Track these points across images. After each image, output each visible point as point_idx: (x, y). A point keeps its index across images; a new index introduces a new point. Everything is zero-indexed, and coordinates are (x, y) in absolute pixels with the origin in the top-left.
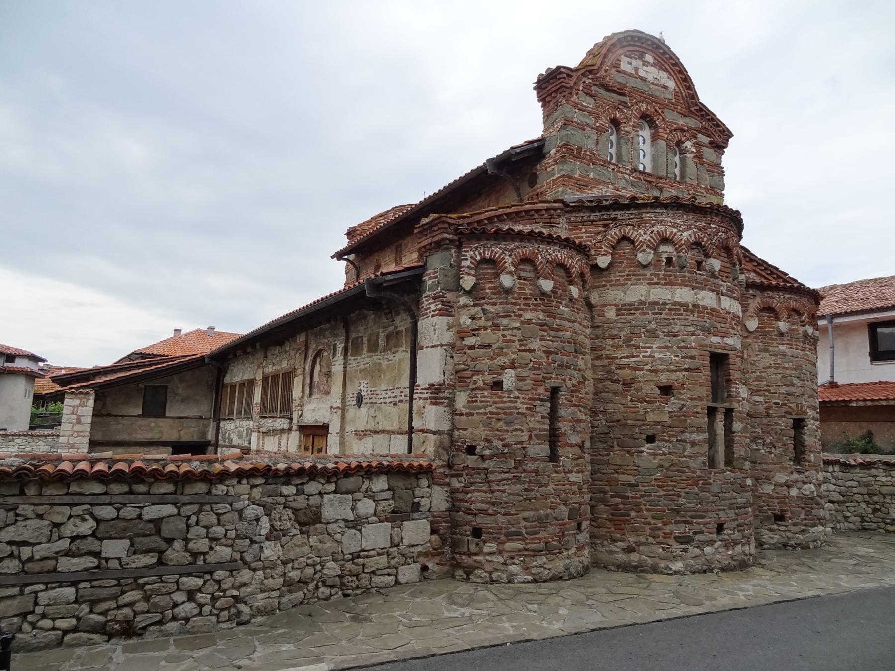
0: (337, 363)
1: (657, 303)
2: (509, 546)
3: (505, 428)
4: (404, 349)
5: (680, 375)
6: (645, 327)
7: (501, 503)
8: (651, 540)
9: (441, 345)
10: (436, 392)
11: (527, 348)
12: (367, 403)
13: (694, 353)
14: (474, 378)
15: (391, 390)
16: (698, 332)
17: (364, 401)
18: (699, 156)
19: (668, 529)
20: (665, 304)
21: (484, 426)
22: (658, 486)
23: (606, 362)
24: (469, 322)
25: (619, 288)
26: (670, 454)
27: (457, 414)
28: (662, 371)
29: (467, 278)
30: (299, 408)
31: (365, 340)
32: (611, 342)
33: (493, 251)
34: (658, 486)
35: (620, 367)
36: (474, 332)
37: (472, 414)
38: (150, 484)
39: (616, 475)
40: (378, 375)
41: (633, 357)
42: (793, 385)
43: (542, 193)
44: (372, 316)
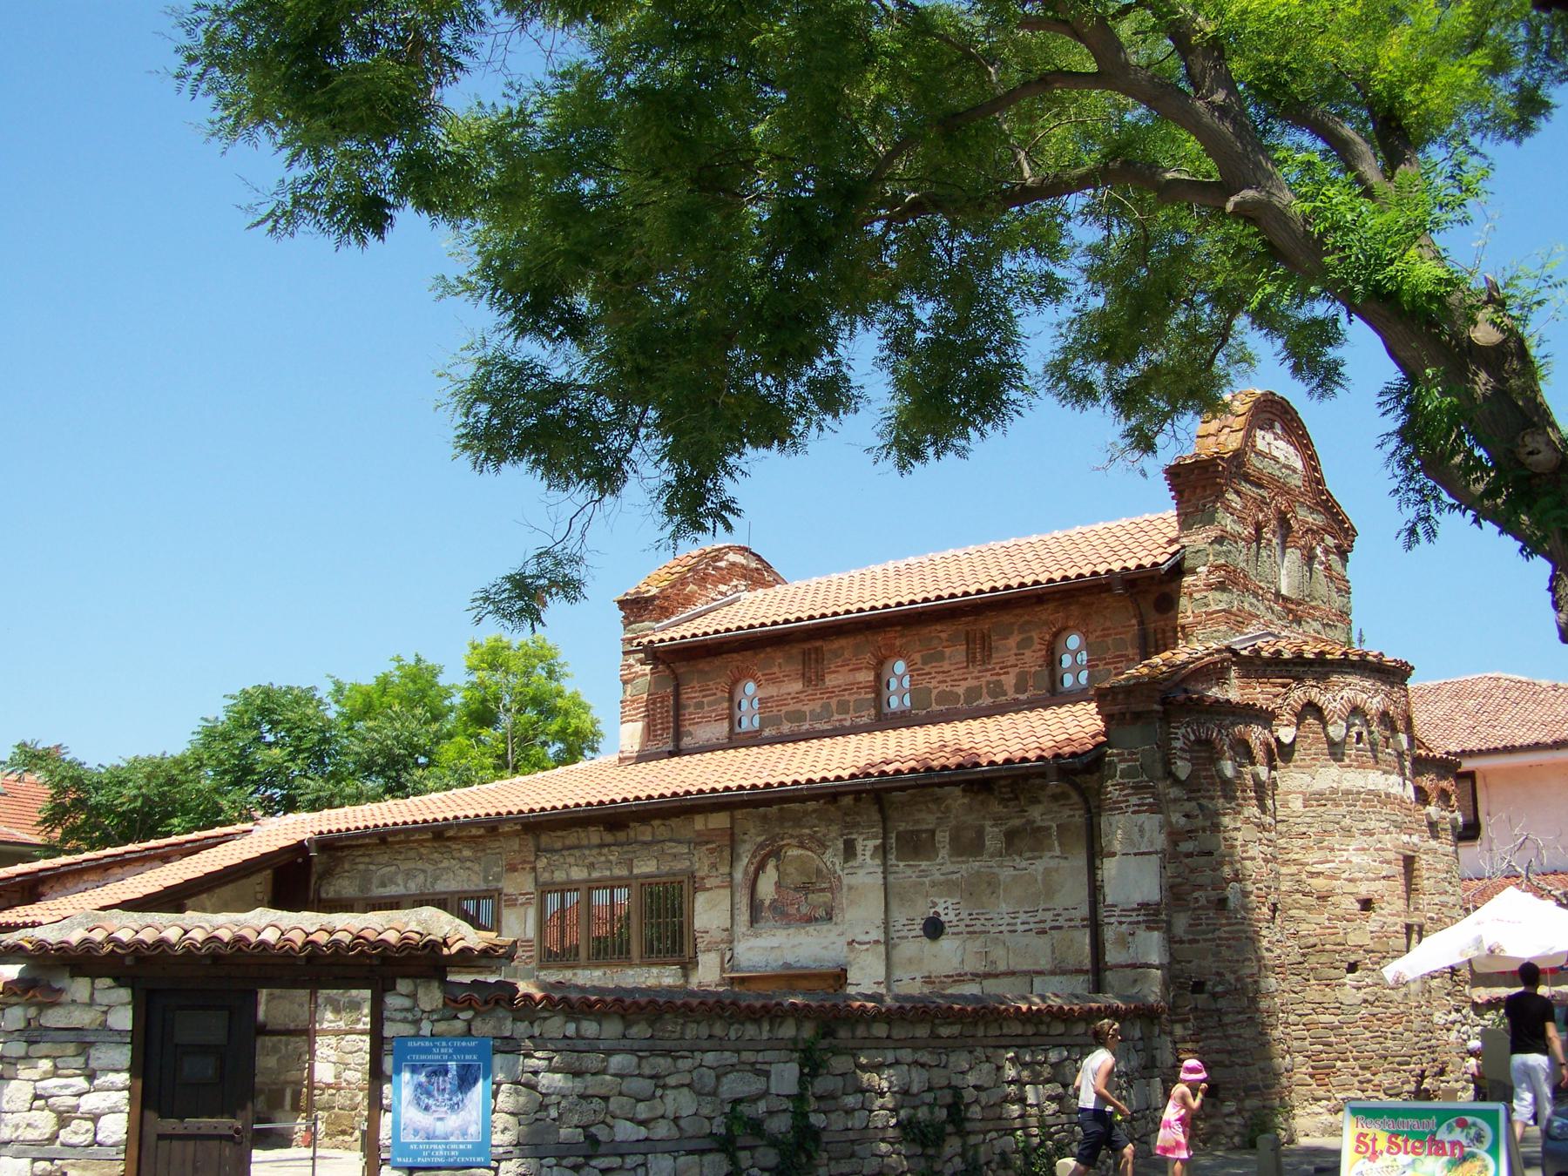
0: (861, 872)
1: (1347, 793)
2: (1248, 1103)
3: (1235, 957)
5: (1380, 885)
6: (1338, 823)
7: (1237, 1051)
8: (1360, 1094)
9: (1156, 853)
10: (1151, 915)
11: (1249, 855)
13: (1391, 855)
14: (1196, 895)
16: (1392, 829)
17: (948, 930)
18: (1328, 568)
19: (1376, 1080)
20: (1359, 793)
21: (1214, 955)
22: (1365, 1028)
23: (1294, 869)
24: (1183, 821)
25: (1305, 770)
26: (1376, 984)
27: (1176, 942)
28: (1361, 880)
29: (1179, 763)
30: (723, 946)
31: (943, 837)
32: (1300, 842)
33: (1208, 729)
34: (1365, 1028)
35: (1312, 875)
36: (1190, 834)
37: (1197, 941)
38: (1048, 1025)
39: (1315, 1016)
41: (1329, 862)
42: (1446, 892)
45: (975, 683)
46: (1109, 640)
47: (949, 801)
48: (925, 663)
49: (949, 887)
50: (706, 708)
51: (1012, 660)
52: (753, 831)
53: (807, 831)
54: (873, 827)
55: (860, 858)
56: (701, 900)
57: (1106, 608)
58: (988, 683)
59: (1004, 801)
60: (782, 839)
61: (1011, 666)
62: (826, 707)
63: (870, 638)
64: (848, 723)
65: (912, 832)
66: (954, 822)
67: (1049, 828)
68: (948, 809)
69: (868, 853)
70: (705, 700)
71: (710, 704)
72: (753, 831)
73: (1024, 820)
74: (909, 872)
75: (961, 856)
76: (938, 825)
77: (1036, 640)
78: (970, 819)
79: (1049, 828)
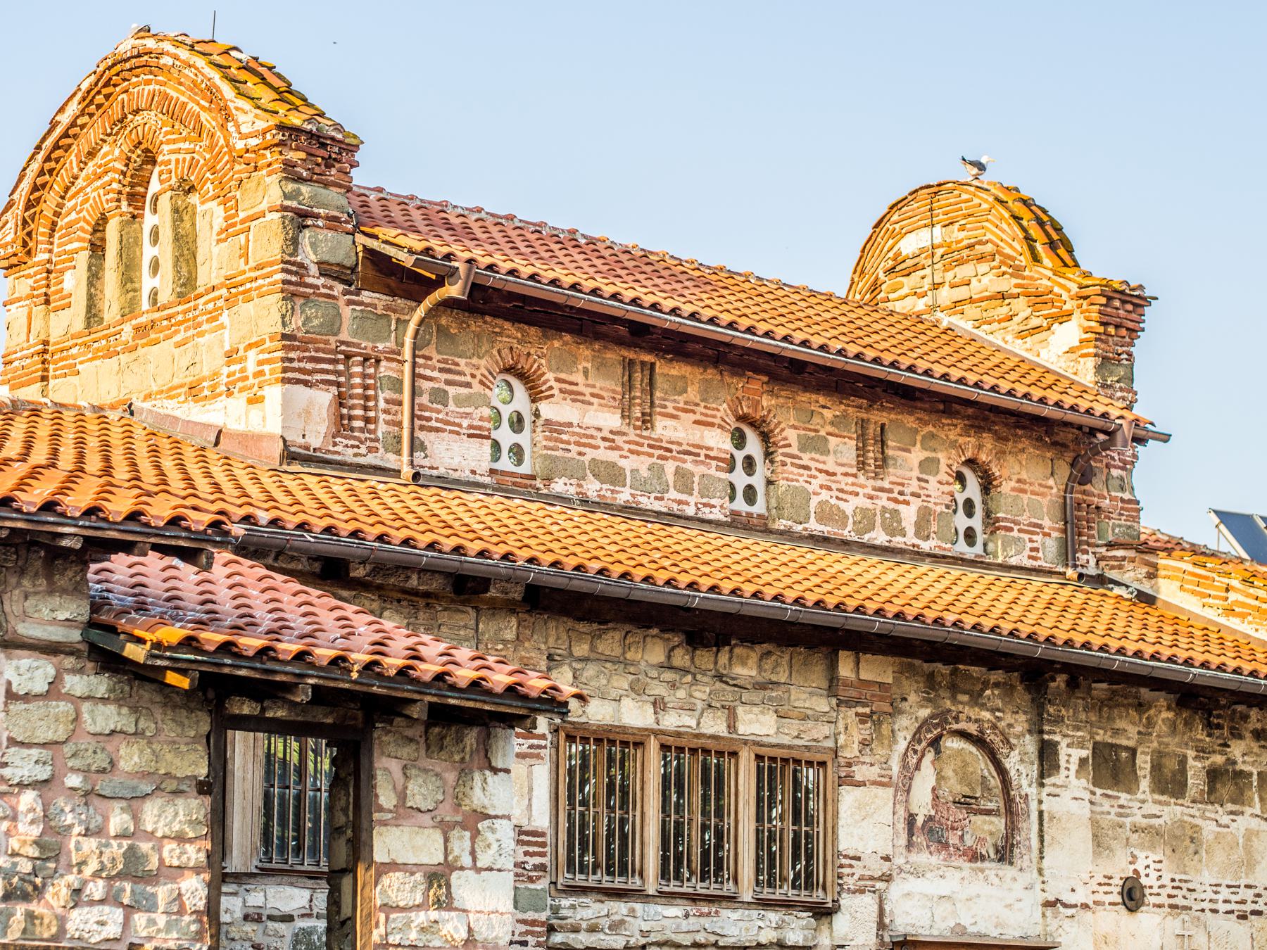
0: (1066, 795)
4: (1258, 812)
12: (1155, 905)
15: (1229, 886)
31: (1144, 762)
40: (1191, 850)
43: (1098, 508)
44: (1163, 715)
45: (867, 503)
46: (1025, 497)
47: (1152, 712)
48: (803, 449)
49: (1151, 834)
50: (451, 406)
51: (914, 486)
52: (913, 698)
53: (986, 715)
54: (1078, 729)
55: (1063, 772)
56: (849, 798)
57: (1023, 450)
58: (884, 509)
59: (1210, 727)
60: (957, 719)
61: (913, 494)
62: (658, 472)
63: (728, 379)
64: (690, 511)
65: (1112, 746)
66: (1155, 744)
67: (1250, 774)
68: (1150, 723)
69: (1074, 767)
70: (452, 391)
71: (459, 401)
72: (913, 698)
73: (1224, 758)
74: (1106, 807)
75: (1162, 793)
76: (1140, 743)
77: (943, 468)
78: (1173, 745)
79: (1250, 774)
